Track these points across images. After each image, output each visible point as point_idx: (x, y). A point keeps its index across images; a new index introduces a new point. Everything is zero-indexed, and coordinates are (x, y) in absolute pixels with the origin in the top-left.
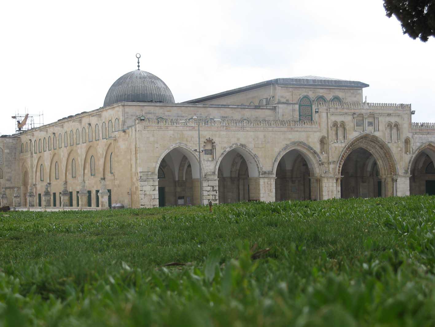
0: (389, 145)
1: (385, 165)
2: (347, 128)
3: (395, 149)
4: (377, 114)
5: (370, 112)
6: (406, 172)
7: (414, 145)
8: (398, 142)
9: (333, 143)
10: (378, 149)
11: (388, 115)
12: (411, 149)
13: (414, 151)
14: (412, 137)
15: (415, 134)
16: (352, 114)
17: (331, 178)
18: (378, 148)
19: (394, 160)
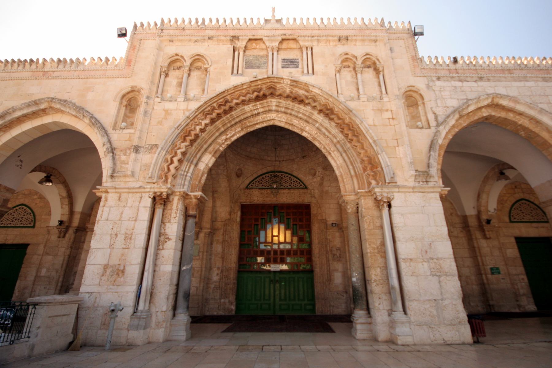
0: (352, 105)
1: (349, 164)
2: (212, 69)
3: (378, 117)
4: (307, 38)
5: (285, 35)
6: (424, 175)
7: (439, 105)
8: (381, 98)
9: (160, 102)
10: (320, 121)
11: (339, 40)
12: (431, 117)
13: (440, 119)
14: (428, 87)
15: (434, 79)
16: (229, 38)
17: (131, 191)
18: (320, 118)
19: (371, 141)
